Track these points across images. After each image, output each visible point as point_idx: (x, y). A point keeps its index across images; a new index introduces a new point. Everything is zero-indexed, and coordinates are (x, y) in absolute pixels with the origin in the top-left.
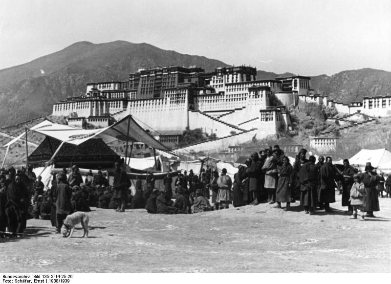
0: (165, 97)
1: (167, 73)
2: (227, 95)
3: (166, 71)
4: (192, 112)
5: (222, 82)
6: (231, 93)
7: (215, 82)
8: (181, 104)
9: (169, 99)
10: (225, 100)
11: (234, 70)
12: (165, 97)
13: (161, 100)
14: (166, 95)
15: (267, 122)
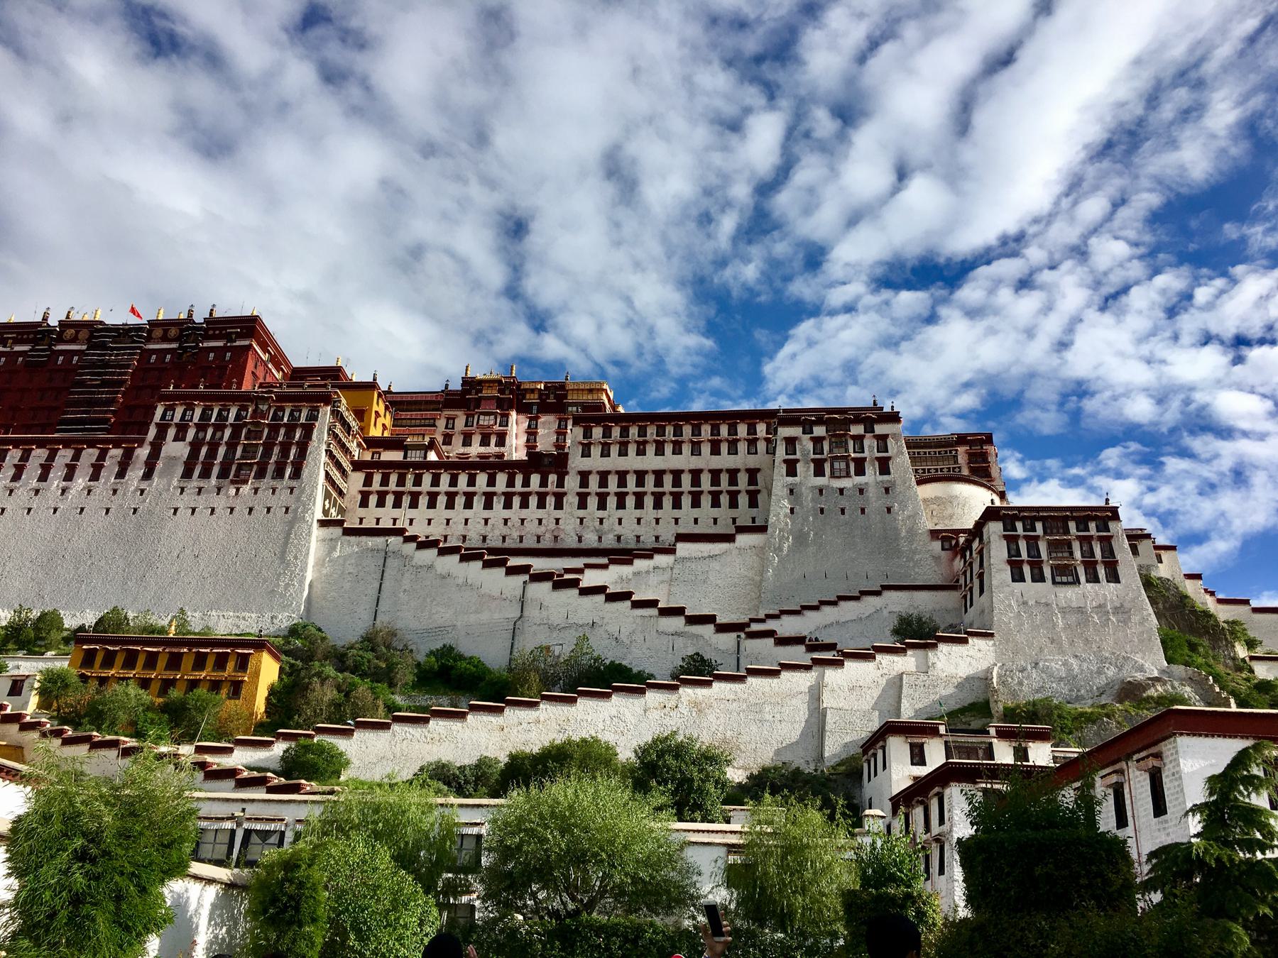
0: (152, 432)
1: (174, 346)
2: (584, 476)
3: (173, 332)
4: (349, 532)
5: (501, 441)
6: (615, 462)
7: (457, 440)
8: (267, 481)
9: (176, 449)
10: (571, 500)
11: (572, 398)
12: (152, 432)
13: (116, 453)
14: (162, 429)
15: (1069, 594)
